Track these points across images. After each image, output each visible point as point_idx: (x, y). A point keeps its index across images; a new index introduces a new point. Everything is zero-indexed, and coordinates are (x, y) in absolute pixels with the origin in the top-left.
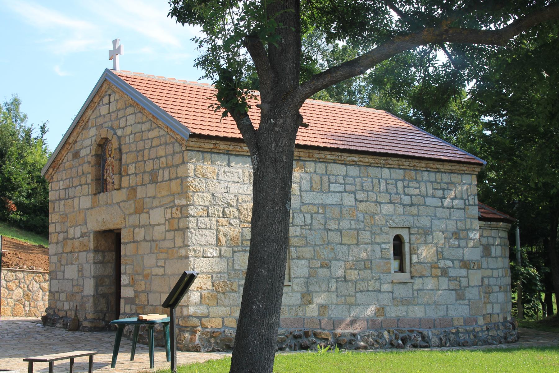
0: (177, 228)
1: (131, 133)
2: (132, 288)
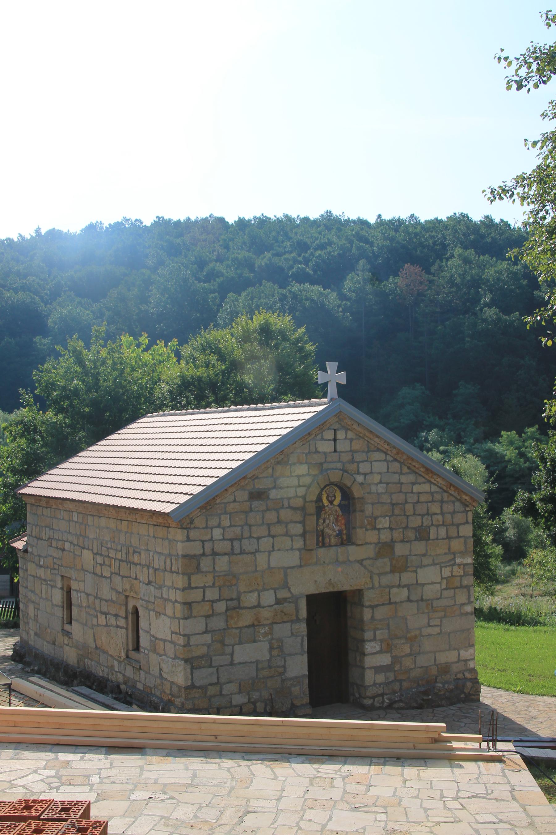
0: (459, 585)
1: (381, 482)
2: (389, 654)
